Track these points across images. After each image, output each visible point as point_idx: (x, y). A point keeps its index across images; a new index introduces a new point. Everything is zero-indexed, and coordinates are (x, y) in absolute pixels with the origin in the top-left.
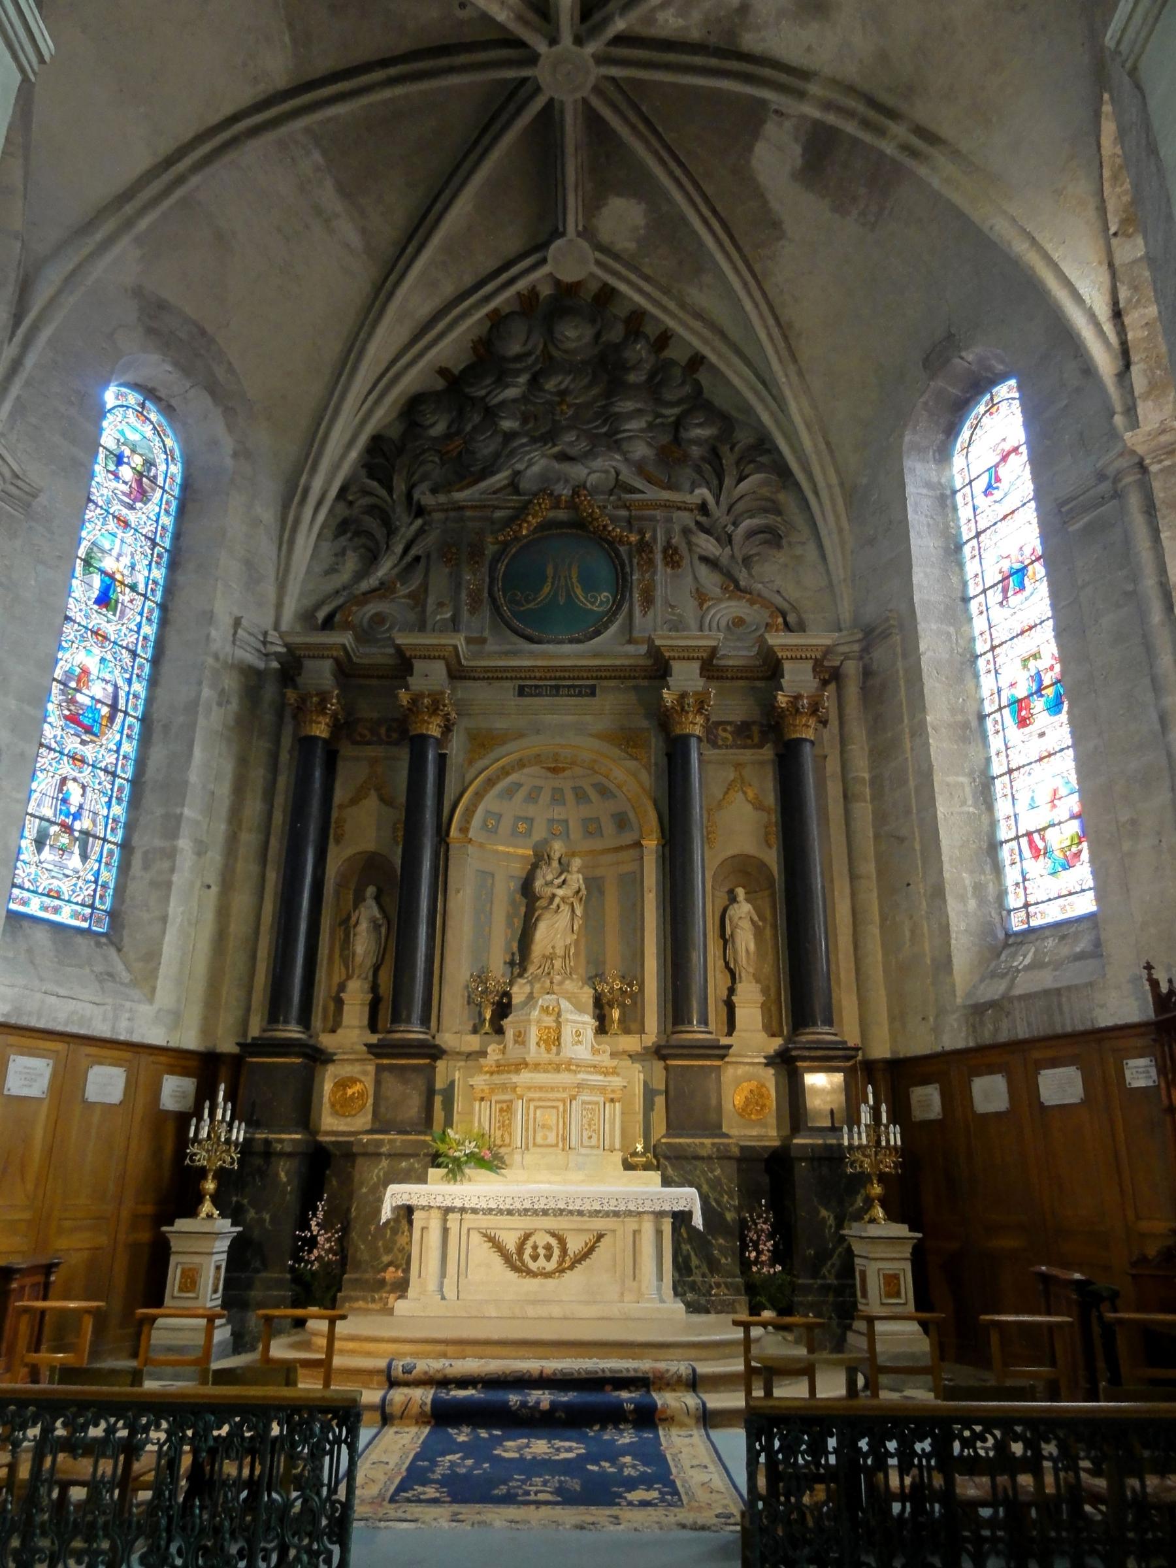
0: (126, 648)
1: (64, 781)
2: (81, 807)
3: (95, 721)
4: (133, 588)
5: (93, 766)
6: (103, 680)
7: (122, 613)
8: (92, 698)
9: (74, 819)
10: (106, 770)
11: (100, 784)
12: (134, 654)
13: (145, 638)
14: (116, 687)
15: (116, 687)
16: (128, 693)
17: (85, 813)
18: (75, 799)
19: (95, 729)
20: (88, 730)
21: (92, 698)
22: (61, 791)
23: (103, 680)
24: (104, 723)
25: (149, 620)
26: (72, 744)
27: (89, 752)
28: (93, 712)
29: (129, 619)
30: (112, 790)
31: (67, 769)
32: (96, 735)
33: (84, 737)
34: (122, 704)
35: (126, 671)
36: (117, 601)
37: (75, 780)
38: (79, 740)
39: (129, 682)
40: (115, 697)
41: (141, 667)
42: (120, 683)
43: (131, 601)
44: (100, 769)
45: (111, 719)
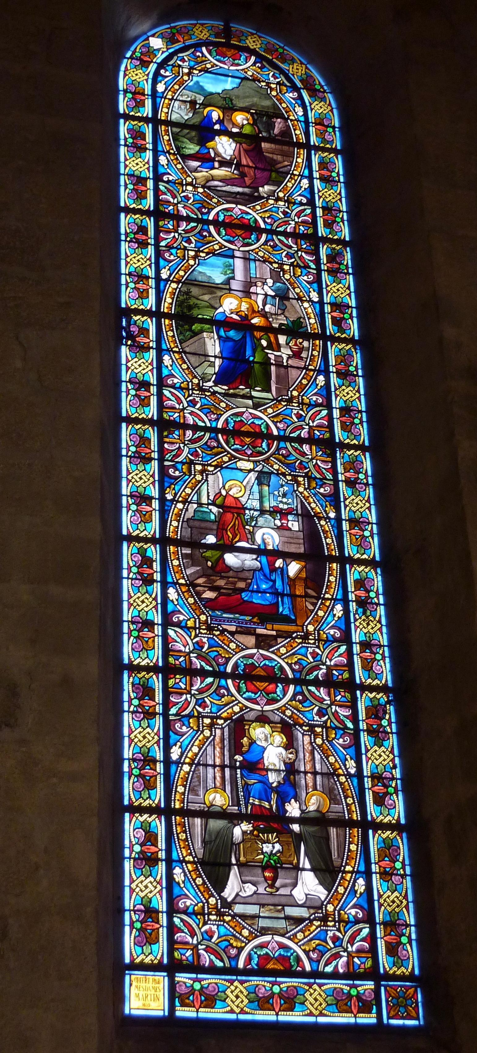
0: (311, 440)
1: (239, 727)
2: (291, 769)
3: (276, 593)
4: (295, 330)
5: (297, 682)
6: (275, 512)
7: (283, 382)
8: (260, 552)
9: (283, 800)
10: (329, 683)
11: (321, 713)
12: (329, 446)
13: (346, 410)
14: (307, 517)
15: (307, 517)
16: (339, 519)
17: (306, 781)
18: (274, 755)
19: (284, 609)
20: (268, 615)
21: (260, 552)
22: (236, 748)
23: (275, 512)
24: (299, 591)
25: (344, 375)
26: (242, 652)
27: (280, 658)
28: (268, 579)
29: (301, 388)
30: (354, 718)
31: (239, 700)
32: (286, 620)
33: (260, 631)
34: (329, 542)
35: (322, 482)
36: (266, 363)
37: (263, 719)
38: (251, 640)
39: (334, 499)
40: (312, 535)
41: (353, 465)
42: (315, 506)
43: (297, 355)
44: (317, 683)
45: (314, 580)
